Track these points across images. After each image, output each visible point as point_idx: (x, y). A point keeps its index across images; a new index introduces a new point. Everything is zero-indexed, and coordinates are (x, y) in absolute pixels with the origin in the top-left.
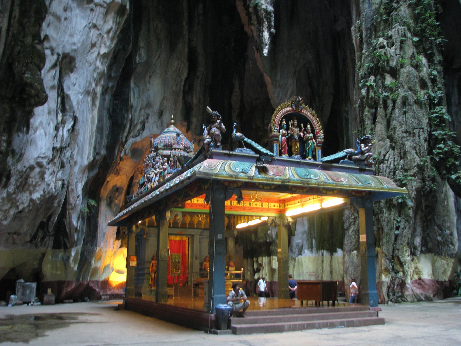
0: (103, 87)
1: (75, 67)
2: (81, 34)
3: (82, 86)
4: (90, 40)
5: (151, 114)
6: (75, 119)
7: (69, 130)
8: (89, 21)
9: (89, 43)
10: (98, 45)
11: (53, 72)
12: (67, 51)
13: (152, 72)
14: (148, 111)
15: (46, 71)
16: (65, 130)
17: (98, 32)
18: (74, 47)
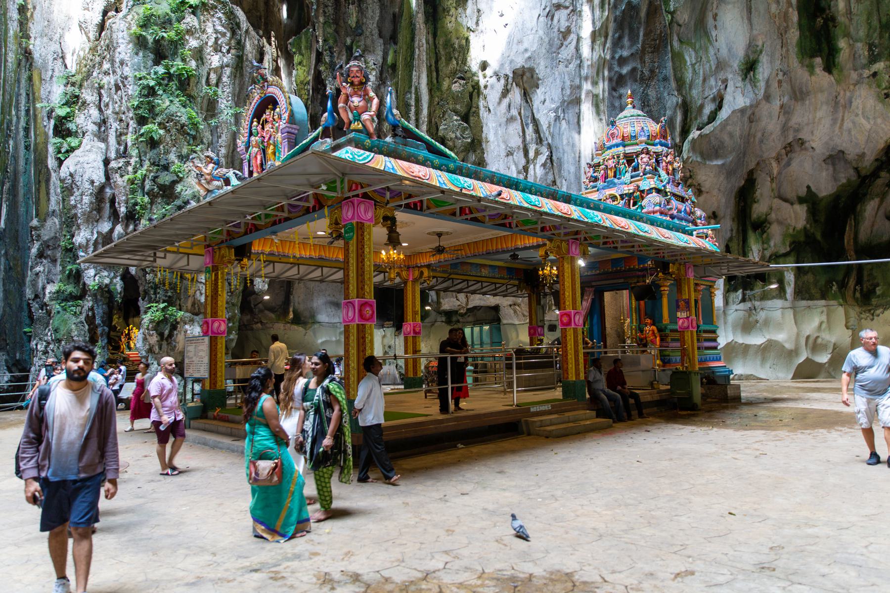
0: (610, 80)
1: (539, 79)
2: (534, 32)
3: (556, 99)
4: (556, 30)
5: (730, 76)
6: (549, 146)
7: (544, 165)
8: (543, 7)
9: (556, 34)
10: (573, 29)
11: (506, 101)
12: (518, 66)
13: (715, 6)
14: (721, 76)
15: (496, 104)
16: (538, 166)
17: (568, 11)
18: (527, 55)
